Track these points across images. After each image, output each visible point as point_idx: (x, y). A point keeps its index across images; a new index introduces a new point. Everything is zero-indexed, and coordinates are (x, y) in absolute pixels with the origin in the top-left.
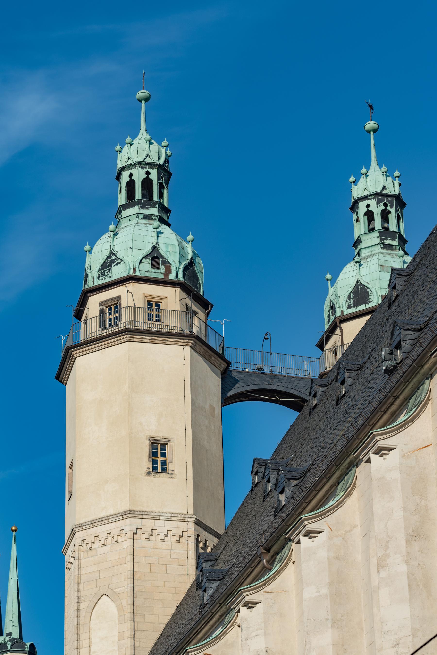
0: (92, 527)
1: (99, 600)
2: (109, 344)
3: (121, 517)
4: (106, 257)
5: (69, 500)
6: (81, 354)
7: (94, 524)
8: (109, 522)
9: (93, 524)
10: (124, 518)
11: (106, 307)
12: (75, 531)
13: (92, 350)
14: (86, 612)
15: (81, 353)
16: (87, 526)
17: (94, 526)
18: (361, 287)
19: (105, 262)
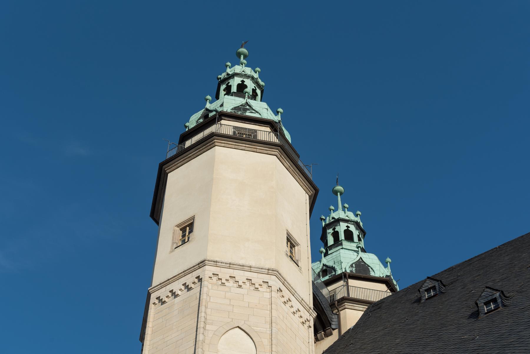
0: (229, 267)
1: (230, 329)
2: (256, 150)
3: (267, 271)
4: (241, 104)
5: (175, 248)
6: (223, 145)
7: (231, 266)
8: (250, 270)
9: (230, 265)
10: (269, 273)
11: (238, 133)
12: (206, 264)
13: (236, 146)
14: (214, 334)
15: (223, 144)
16: (222, 264)
17: (230, 268)
18: (363, 263)
19: (239, 106)
